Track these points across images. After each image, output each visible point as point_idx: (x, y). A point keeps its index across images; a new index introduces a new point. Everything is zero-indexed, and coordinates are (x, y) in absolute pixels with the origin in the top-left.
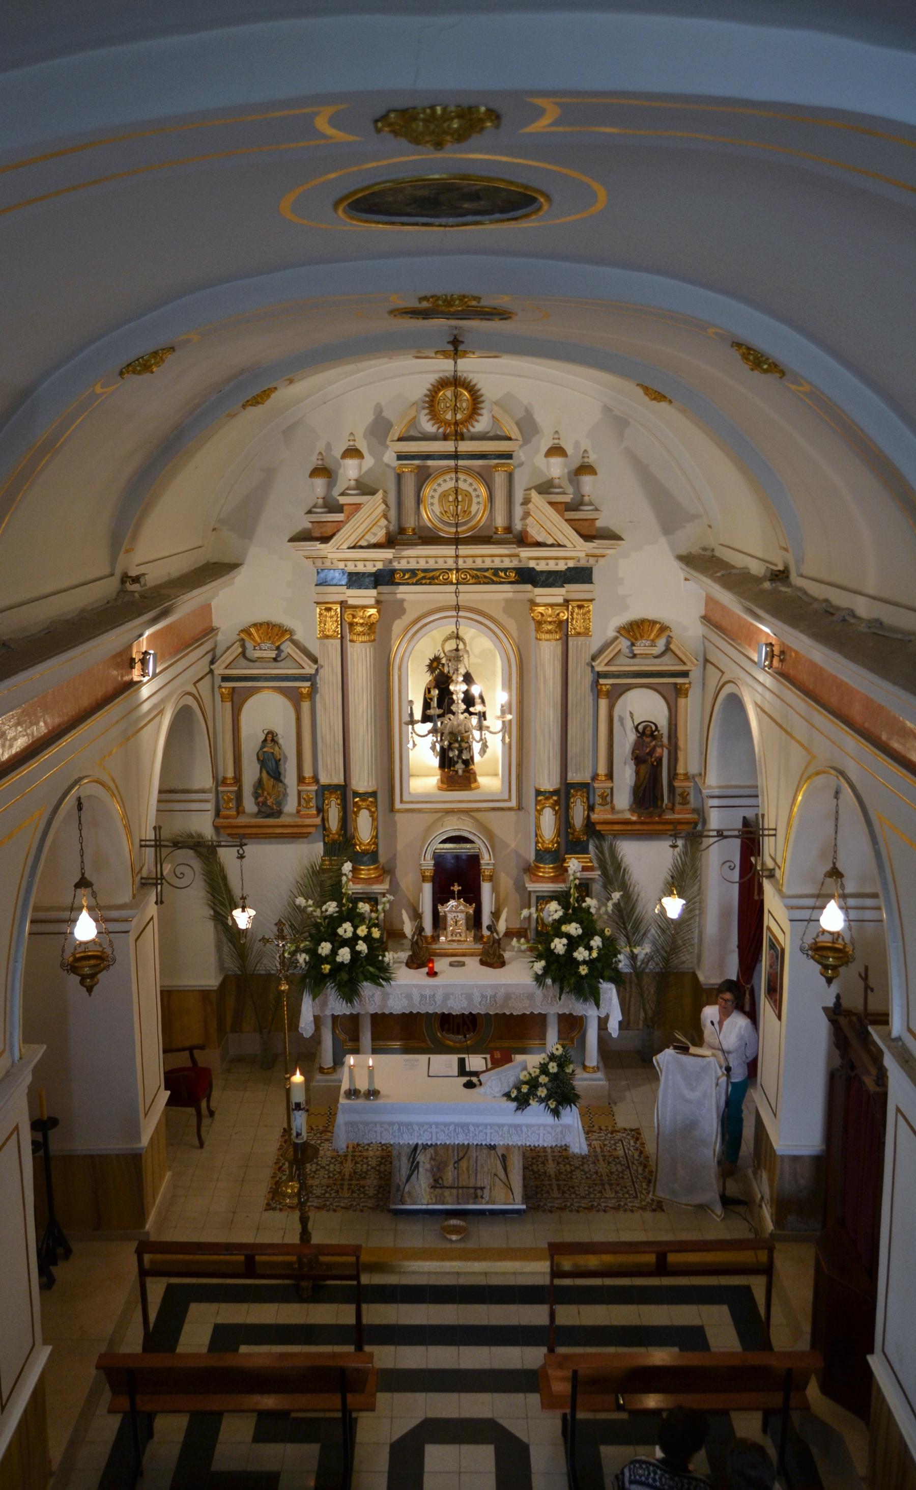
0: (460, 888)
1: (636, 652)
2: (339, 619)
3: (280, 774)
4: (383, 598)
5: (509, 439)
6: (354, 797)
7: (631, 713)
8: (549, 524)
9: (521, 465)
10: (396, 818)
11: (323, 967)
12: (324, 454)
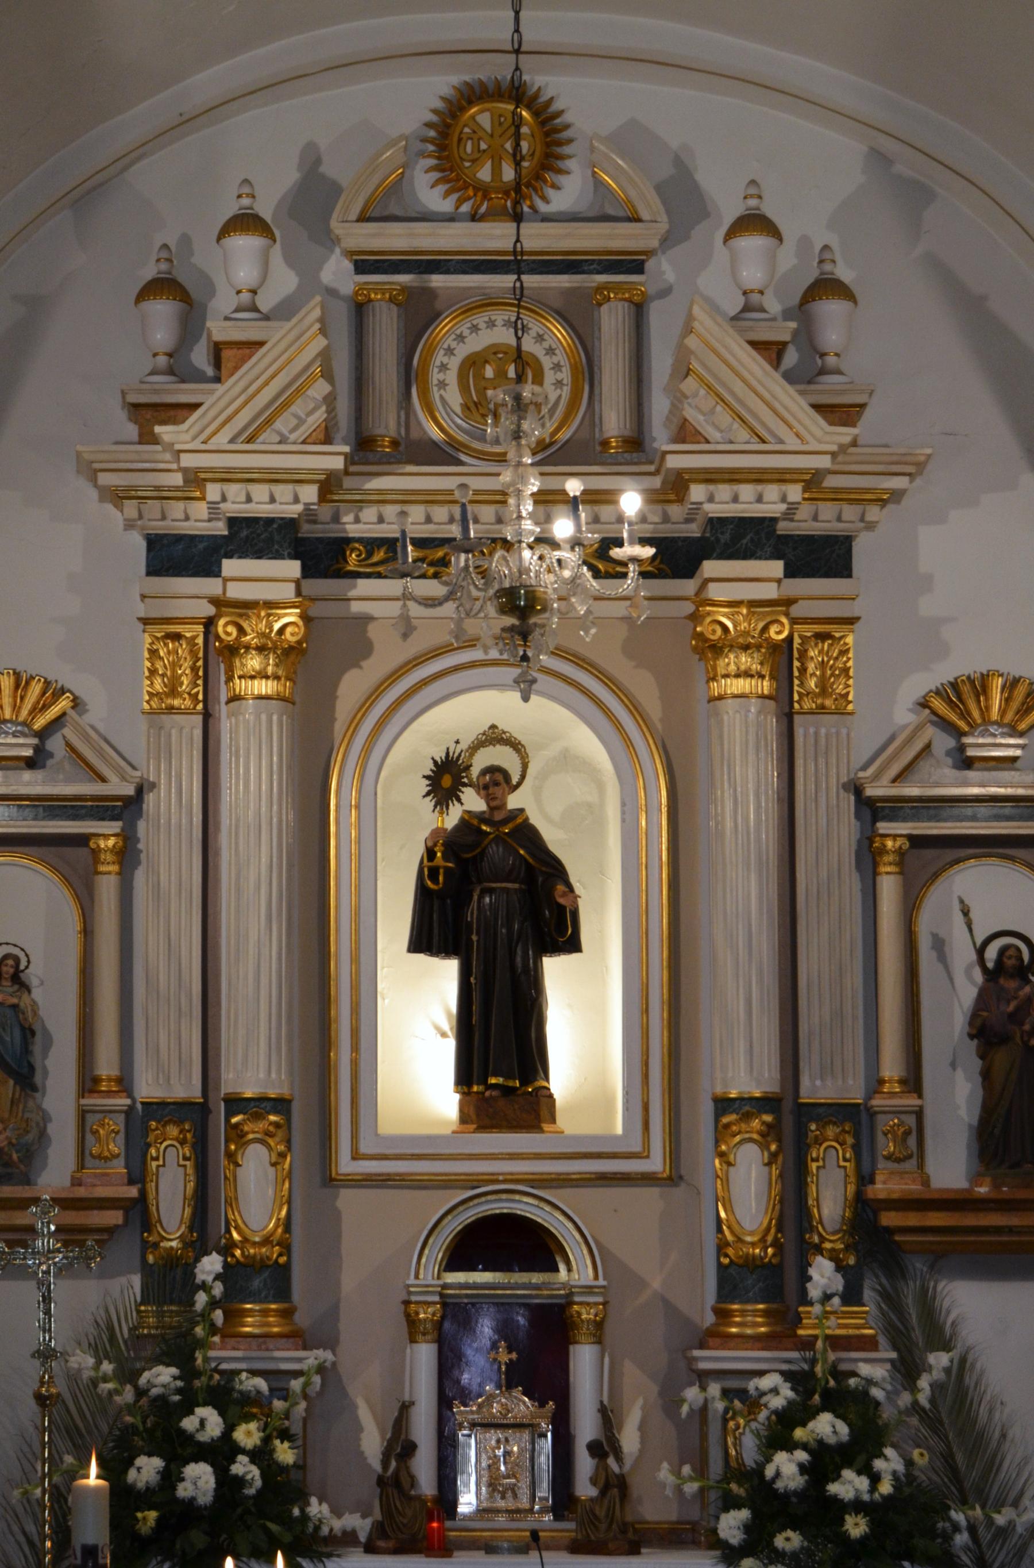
0: (514, 1356)
1: (971, 752)
2: (200, 663)
3: (32, 1068)
4: (315, 610)
5: (638, 220)
6: (229, 1115)
7: (962, 901)
8: (739, 387)
9: (665, 292)
10: (339, 1204)
11: (139, 1515)
12: (173, 249)
